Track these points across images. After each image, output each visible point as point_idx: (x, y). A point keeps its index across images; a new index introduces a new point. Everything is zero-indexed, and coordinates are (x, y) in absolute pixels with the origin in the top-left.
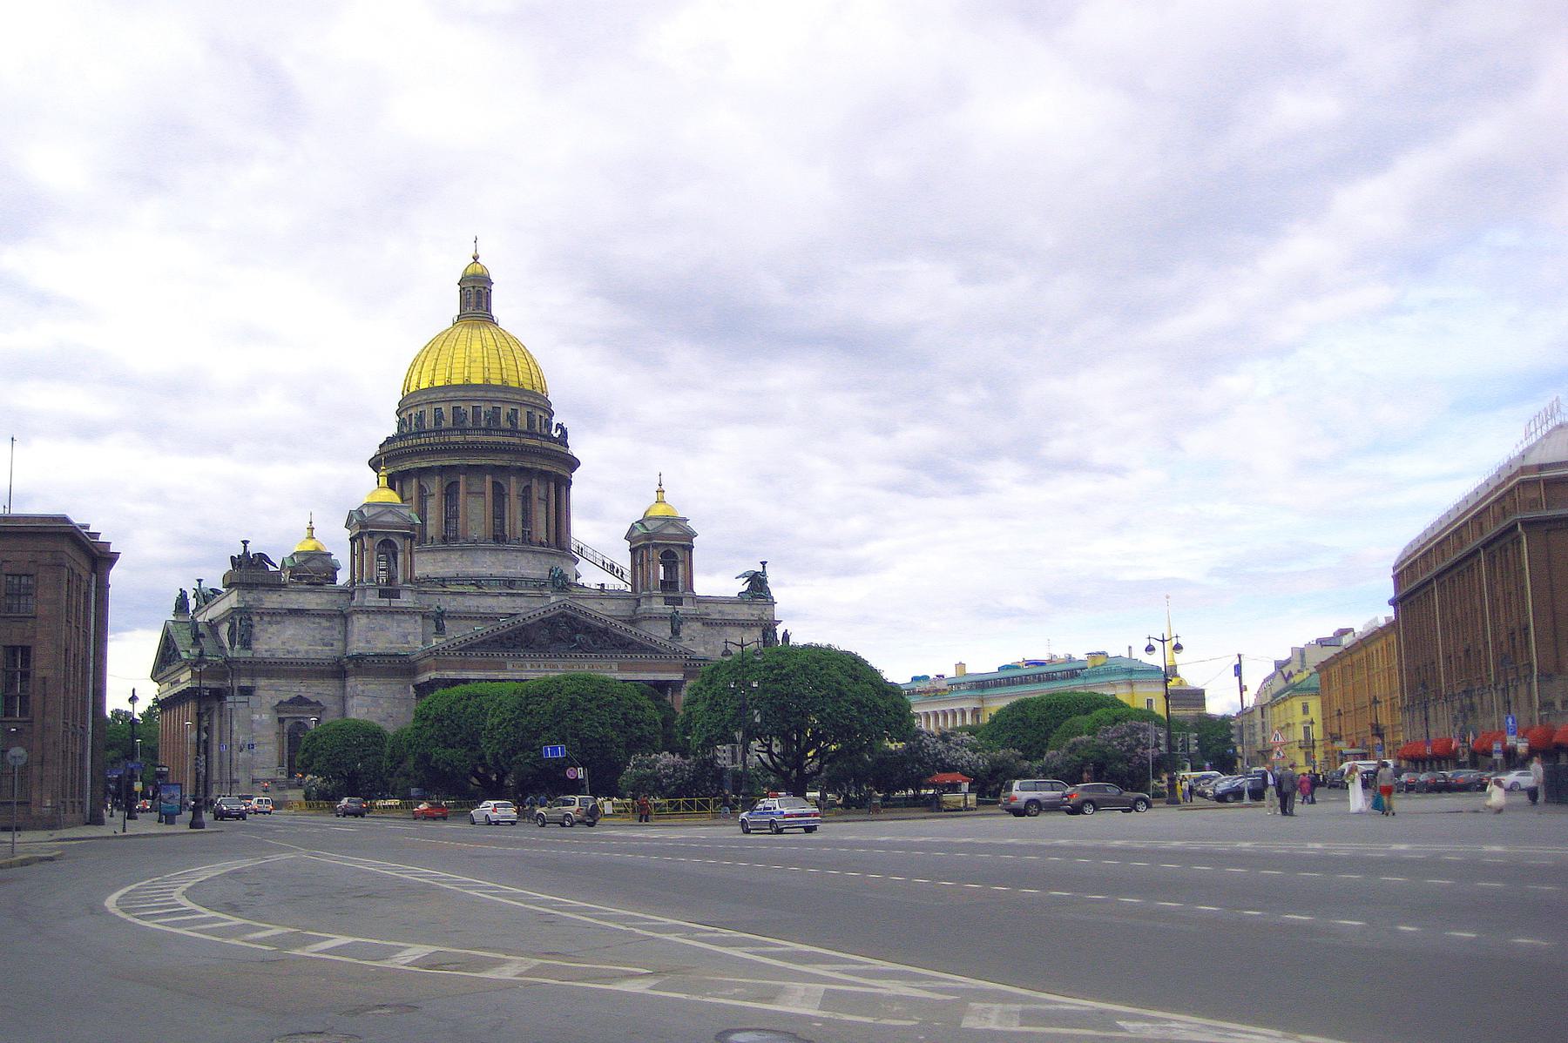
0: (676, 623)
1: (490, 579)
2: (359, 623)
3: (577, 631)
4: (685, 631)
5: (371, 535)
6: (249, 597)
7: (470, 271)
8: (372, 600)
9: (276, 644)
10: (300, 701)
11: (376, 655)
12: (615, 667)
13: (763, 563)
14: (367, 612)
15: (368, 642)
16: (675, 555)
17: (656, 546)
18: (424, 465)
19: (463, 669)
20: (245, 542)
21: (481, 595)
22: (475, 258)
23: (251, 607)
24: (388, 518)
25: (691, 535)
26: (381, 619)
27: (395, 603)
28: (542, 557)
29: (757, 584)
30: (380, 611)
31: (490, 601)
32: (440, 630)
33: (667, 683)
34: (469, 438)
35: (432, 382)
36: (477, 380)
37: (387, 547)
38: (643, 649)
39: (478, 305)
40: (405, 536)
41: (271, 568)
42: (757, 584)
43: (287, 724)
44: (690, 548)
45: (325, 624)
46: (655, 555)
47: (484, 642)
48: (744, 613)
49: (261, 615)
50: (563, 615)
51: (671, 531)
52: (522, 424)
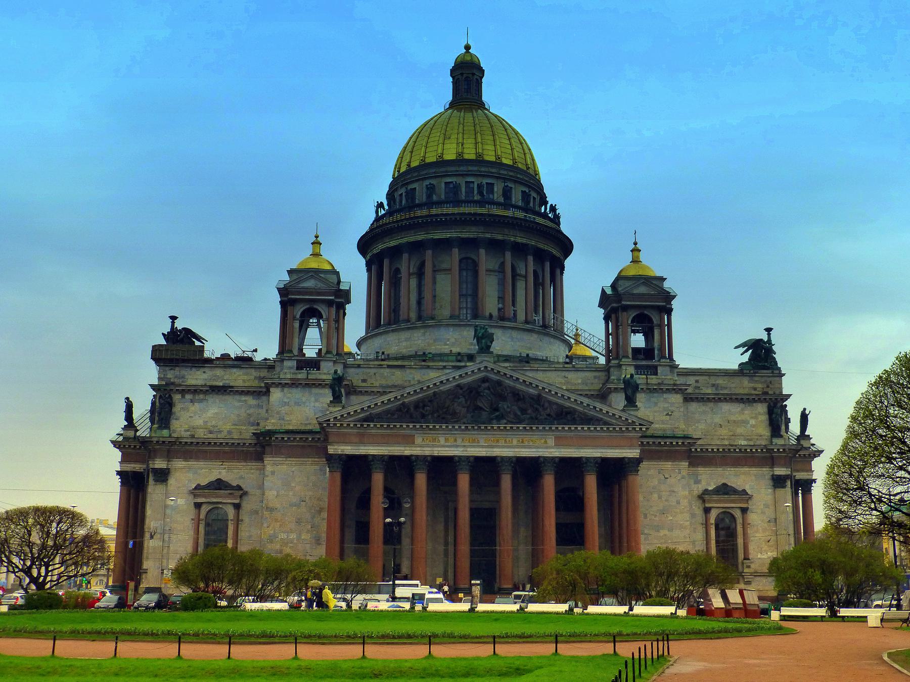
0: (631, 391)
1: (441, 356)
2: (276, 395)
3: (503, 398)
4: (641, 399)
6: (171, 375)
7: (459, 60)
8: (288, 371)
9: (199, 422)
10: (219, 485)
12: (551, 441)
13: (769, 330)
14: (282, 386)
16: (650, 320)
17: (626, 308)
18: (393, 243)
19: (361, 442)
20: (173, 318)
21: (422, 367)
22: (467, 48)
23: (173, 384)
24: (310, 284)
25: (669, 297)
26: (296, 394)
27: (314, 374)
28: (515, 334)
29: (761, 354)
30: (294, 384)
31: (433, 374)
32: (337, 399)
33: (620, 461)
34: (434, 211)
35: (409, 165)
36: (450, 156)
38: (588, 420)
40: (330, 303)
41: (197, 343)
42: (761, 354)
43: (204, 509)
44: (669, 311)
45: (251, 401)
46: (627, 318)
47: (387, 412)
48: (745, 386)
49: (183, 392)
50: (485, 380)
51: (642, 290)
52: (498, 196)
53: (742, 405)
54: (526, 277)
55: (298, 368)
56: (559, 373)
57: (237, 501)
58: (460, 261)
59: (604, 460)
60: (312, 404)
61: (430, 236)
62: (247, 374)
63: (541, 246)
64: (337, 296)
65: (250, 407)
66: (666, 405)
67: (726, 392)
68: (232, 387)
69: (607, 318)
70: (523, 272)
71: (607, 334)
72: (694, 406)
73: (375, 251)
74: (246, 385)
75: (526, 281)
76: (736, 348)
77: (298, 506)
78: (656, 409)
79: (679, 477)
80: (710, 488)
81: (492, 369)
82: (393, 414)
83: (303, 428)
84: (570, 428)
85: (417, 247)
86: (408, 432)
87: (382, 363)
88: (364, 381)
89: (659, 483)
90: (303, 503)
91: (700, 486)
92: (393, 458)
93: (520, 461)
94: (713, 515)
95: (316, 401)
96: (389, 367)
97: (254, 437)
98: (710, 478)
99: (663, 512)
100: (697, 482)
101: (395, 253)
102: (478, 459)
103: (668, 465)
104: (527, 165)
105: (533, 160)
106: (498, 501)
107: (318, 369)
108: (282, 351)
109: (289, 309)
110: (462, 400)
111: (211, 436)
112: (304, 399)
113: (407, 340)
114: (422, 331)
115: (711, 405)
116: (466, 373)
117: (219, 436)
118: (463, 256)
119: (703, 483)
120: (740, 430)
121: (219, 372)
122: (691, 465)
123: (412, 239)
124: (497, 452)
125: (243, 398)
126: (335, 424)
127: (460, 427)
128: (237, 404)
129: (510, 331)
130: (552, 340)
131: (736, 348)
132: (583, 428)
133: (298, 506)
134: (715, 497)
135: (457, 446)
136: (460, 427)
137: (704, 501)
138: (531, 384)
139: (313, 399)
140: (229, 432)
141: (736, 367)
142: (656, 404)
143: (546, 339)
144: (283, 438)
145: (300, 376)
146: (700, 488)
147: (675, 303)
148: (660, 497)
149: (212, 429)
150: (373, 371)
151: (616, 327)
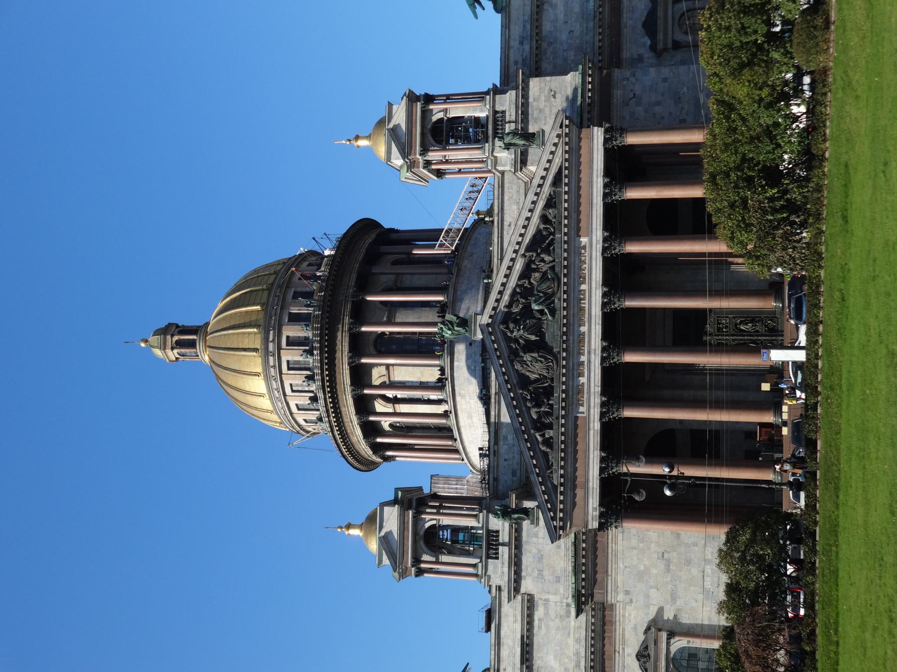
5: (417, 561)
8: (499, 571)
10: (643, 655)
11: (576, 571)
15: (558, 580)
16: (440, 121)
18: (358, 432)
25: (412, 98)
26: (527, 560)
27: (504, 537)
30: (516, 563)
35: (271, 412)
37: (432, 540)
39: (192, 344)
44: (429, 99)
45: (539, 614)
53: (546, 7)
54: (397, 274)
55: (497, 558)
56: (505, 233)
57: (664, 635)
58: (380, 354)
59: (608, 172)
60: (540, 540)
61: (348, 389)
62: (507, 615)
63: (361, 257)
64: (409, 508)
65: (547, 614)
66: (543, 98)
67: (528, 26)
68: (522, 637)
69: (439, 174)
70: (392, 277)
71: (460, 171)
72: (545, 65)
73: (370, 452)
74: (519, 618)
75: (403, 274)
76: (476, 17)
77: (668, 563)
78: (547, 110)
79: (633, 79)
80: (649, 42)
81: (491, 317)
82: (548, 442)
83: (571, 553)
84: (566, 218)
85: (364, 406)
86: (571, 425)
87: (492, 450)
88: (514, 473)
89: (638, 104)
90: (666, 556)
91: (646, 56)
92: (605, 446)
93: (609, 279)
94: (680, 37)
95: (536, 535)
96: (496, 442)
97: (583, 617)
98: (635, 42)
99: (678, 99)
100: (640, 59)
101: (371, 430)
102: (607, 335)
103: (618, 94)
104: (270, 274)
105: (267, 266)
106: (665, 310)
107: (498, 532)
108: (476, 575)
109: (423, 566)
110: (527, 357)
111: (583, 664)
112: (534, 551)
113: (470, 417)
114: (458, 398)
115: (544, 45)
116: (496, 350)
117: (583, 655)
118: (372, 350)
119: (641, 51)
120: (577, 9)
121: (504, 653)
122: (619, 65)
123: (352, 409)
124: (596, 311)
125: (536, 623)
126: (561, 519)
127: (564, 359)
128: (543, 631)
129: (459, 293)
130: (472, 242)
131: (476, 17)
132: (566, 201)
133: (668, 563)
134: (660, 36)
135: (589, 361)
136: (564, 359)
137: (665, 50)
138: (510, 268)
139: (534, 540)
140: (578, 641)
141: (499, 16)
142: (541, 111)
143: (469, 249)
144: (583, 579)
145: (506, 556)
146: (648, 55)
147: (419, 92)
148: (658, 103)
149: (573, 664)
150: (502, 463)
151: (447, 162)
